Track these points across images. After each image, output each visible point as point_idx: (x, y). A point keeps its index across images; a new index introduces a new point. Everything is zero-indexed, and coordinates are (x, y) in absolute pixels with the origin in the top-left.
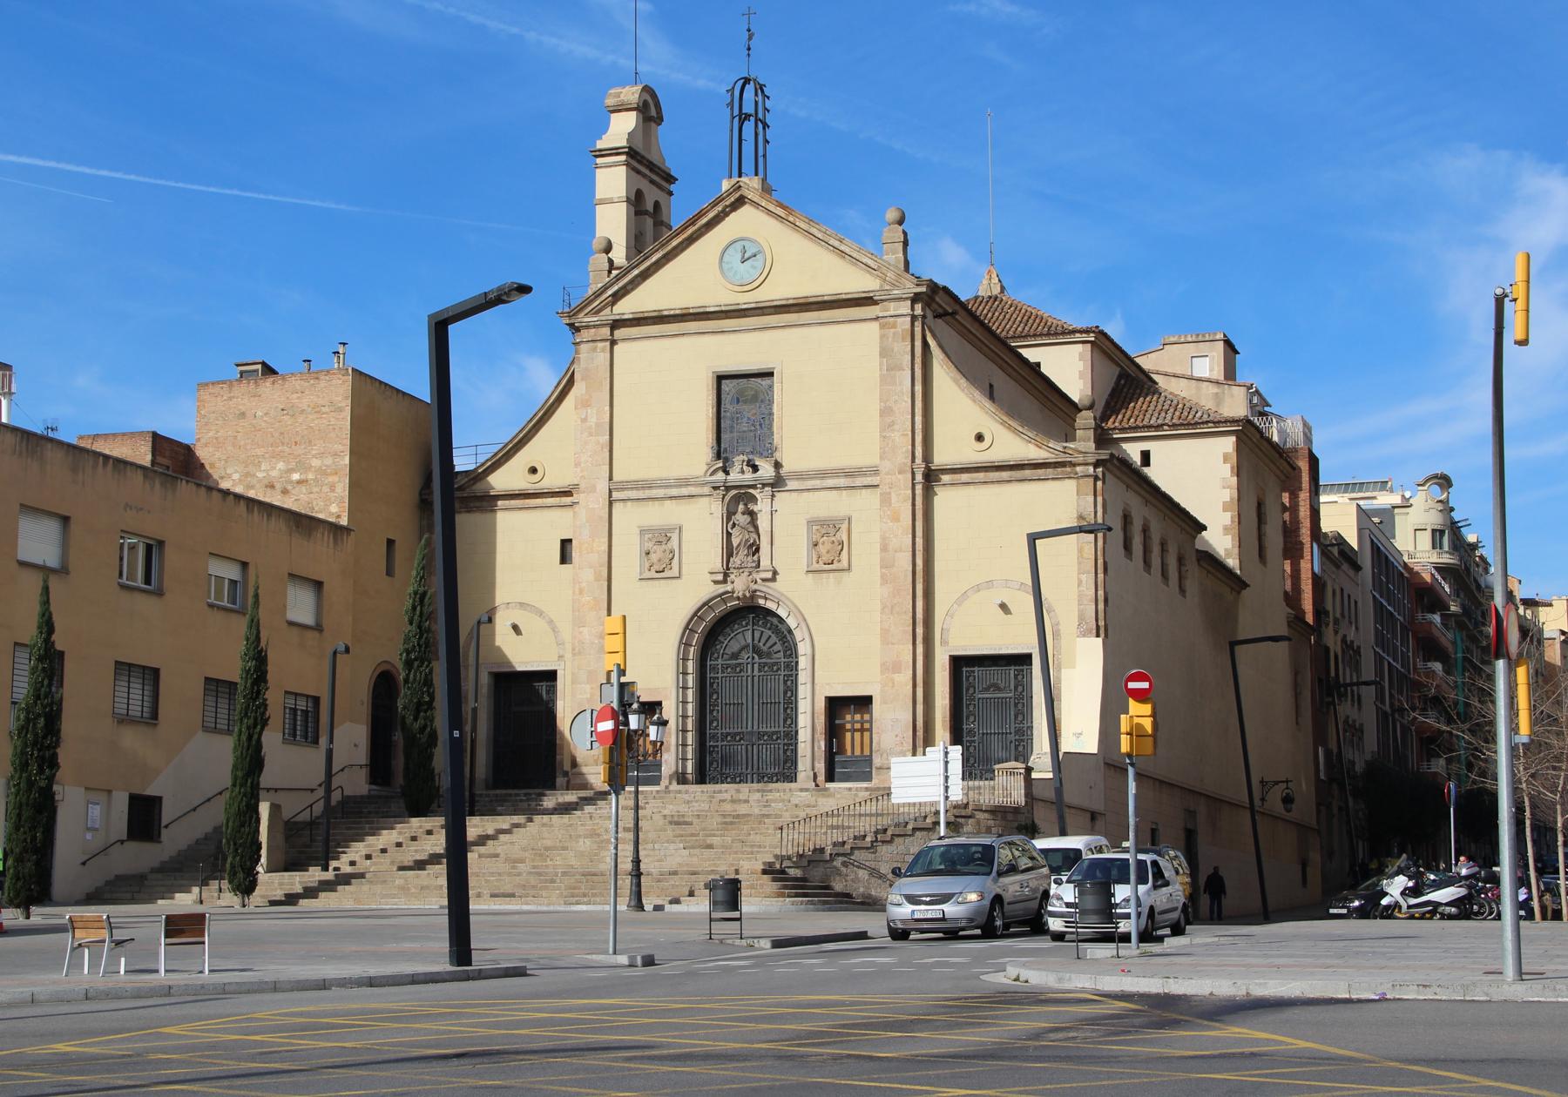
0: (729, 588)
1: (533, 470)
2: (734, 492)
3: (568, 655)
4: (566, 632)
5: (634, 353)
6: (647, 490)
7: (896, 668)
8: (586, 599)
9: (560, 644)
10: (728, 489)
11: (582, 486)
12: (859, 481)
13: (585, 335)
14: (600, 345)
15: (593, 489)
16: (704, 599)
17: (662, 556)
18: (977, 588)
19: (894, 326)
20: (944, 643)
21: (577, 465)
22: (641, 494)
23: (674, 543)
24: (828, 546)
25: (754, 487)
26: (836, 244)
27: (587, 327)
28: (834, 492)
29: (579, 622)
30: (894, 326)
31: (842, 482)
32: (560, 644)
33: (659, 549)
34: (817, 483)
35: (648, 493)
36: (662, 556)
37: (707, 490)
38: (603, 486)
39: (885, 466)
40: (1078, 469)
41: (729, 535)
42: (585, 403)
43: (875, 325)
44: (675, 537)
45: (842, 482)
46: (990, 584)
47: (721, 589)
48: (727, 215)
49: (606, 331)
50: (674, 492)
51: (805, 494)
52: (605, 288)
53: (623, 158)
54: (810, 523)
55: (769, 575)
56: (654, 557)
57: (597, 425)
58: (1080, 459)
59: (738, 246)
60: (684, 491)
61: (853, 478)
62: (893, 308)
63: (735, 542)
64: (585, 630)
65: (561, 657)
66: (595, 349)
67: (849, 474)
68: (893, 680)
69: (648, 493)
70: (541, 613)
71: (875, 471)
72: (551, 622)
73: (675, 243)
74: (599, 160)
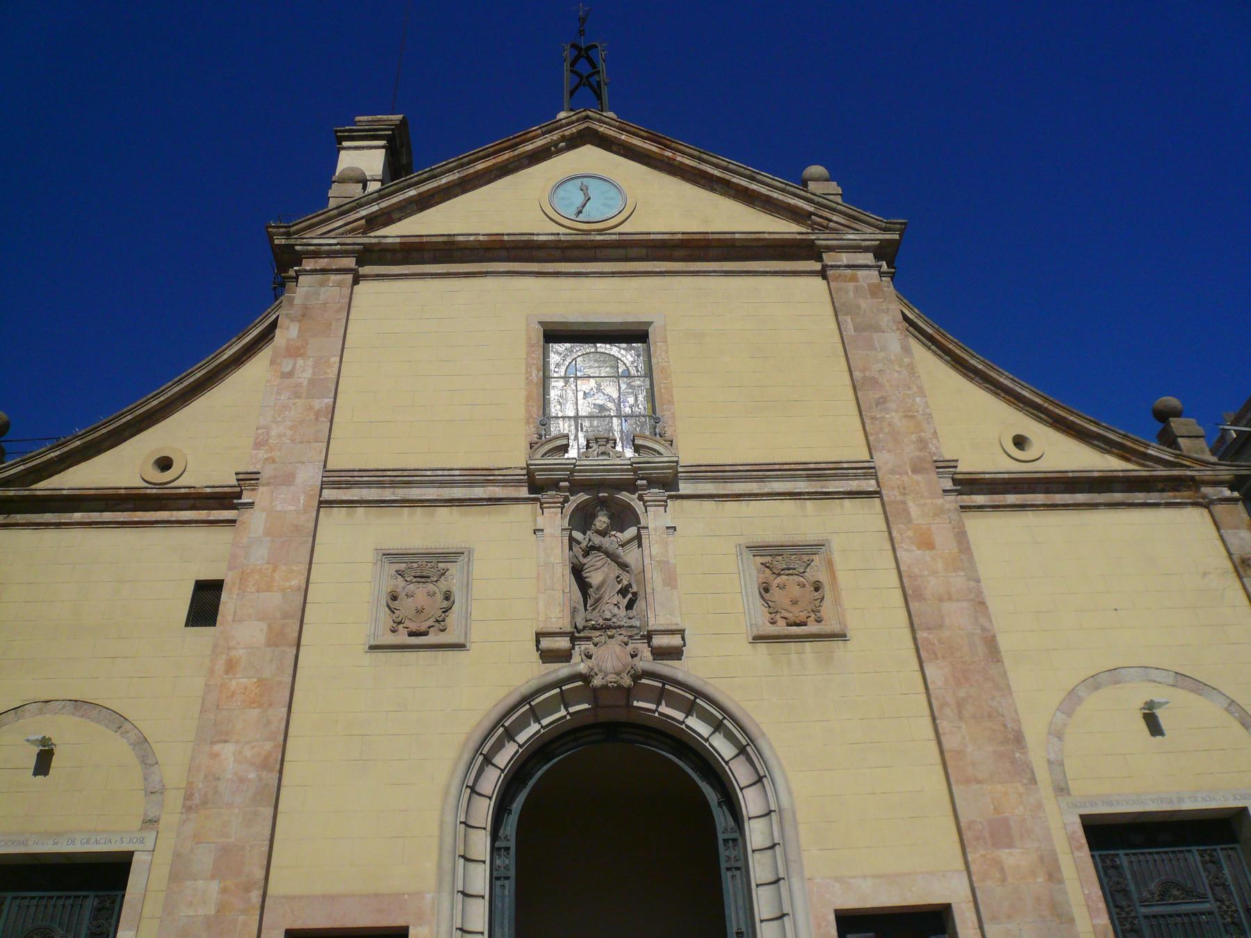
0: (582, 668)
1: (164, 464)
2: (582, 497)
3: (170, 817)
4: (173, 767)
5: (386, 302)
6: (393, 488)
7: (1001, 834)
8: (240, 681)
9: (154, 792)
10: (576, 486)
11: (264, 477)
12: (833, 486)
13: (308, 264)
14: (333, 277)
15: (289, 479)
16: (525, 690)
17: (421, 609)
18: (1094, 682)
19: (854, 279)
20: (1062, 790)
21: (258, 445)
22: (388, 494)
23: (454, 580)
24: (796, 591)
25: (631, 487)
26: (744, 182)
27: (316, 255)
28: (789, 506)
29: (214, 731)
30: (854, 279)
31: (802, 486)
32: (154, 792)
33: (421, 593)
34: (753, 487)
35: (401, 493)
36: (421, 609)
37: (524, 492)
38: (310, 476)
39: (883, 460)
40: (1205, 490)
41: (577, 572)
42: (295, 352)
43: (818, 282)
44: (454, 569)
45: (802, 486)
46: (1114, 675)
47: (563, 670)
48: (560, 151)
49: (350, 262)
50: (458, 493)
51: (731, 506)
52: (359, 204)
53: (382, 143)
54: (757, 549)
55: (675, 641)
56: (406, 607)
57: (311, 381)
58: (1208, 474)
59: (578, 182)
60: (478, 492)
61: (820, 480)
62: (845, 258)
63: (595, 578)
64: (227, 751)
65: (150, 823)
66: (322, 284)
67: (815, 472)
68: (998, 864)
69: (401, 493)
70: (118, 721)
71: (869, 471)
72: (142, 743)
73: (480, 166)
74: (345, 144)
